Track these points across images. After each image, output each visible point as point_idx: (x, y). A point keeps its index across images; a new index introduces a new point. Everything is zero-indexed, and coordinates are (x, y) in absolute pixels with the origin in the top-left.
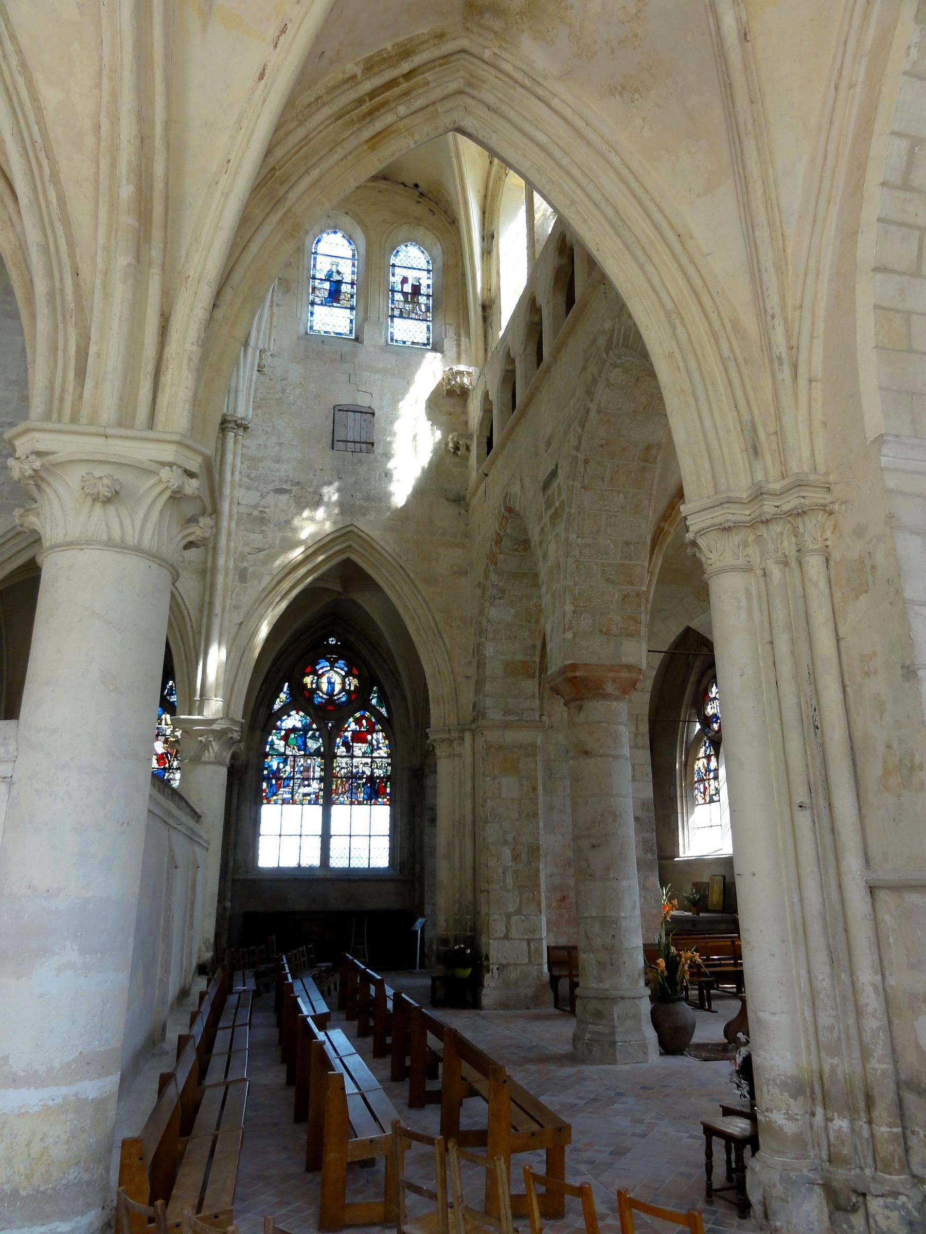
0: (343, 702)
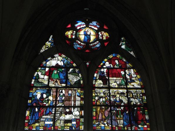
0: (98, 48)
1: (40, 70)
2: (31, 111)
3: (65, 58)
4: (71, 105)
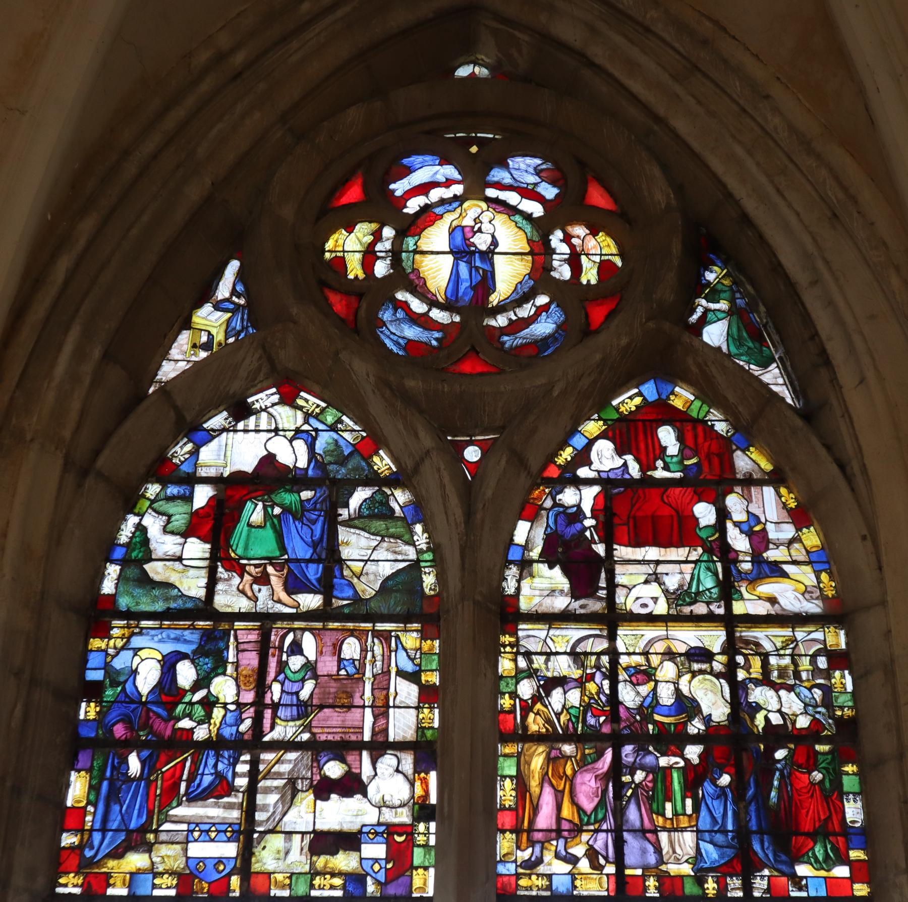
0: (545, 341)
1: (153, 502)
2: (95, 773)
3: (316, 417)
4: (353, 738)
